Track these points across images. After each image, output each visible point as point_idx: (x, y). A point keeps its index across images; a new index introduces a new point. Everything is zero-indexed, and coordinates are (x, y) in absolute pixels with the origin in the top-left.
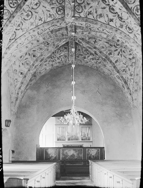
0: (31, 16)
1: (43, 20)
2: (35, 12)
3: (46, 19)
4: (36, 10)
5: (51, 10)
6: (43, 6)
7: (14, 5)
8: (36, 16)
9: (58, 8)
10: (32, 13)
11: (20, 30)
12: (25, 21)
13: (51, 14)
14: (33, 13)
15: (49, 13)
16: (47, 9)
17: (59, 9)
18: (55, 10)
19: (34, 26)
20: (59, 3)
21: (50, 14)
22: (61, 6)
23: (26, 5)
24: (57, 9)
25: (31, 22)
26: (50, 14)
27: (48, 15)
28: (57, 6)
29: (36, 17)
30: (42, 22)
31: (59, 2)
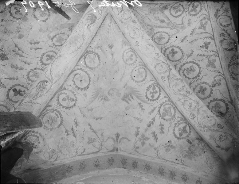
0: (194, 65)
1: (208, 40)
2: (190, 56)
3: (208, 35)
4: (185, 55)
5: (193, 26)
6: (182, 41)
7: (156, 92)
8: (198, 55)
9: (191, 13)
10: (187, 63)
11: (213, 88)
12: (200, 78)
13: (199, 25)
14: (189, 59)
15: (197, 31)
16: (189, 34)
17: (192, 11)
18: (193, 19)
19: (215, 60)
20: (183, 11)
21: (199, 28)
22: (188, 8)
23: (155, 67)
24: (192, 15)
25: (207, 66)
26: (199, 28)
27: (202, 30)
28: (188, 15)
29: (201, 55)
30: (212, 42)
31: (181, 12)
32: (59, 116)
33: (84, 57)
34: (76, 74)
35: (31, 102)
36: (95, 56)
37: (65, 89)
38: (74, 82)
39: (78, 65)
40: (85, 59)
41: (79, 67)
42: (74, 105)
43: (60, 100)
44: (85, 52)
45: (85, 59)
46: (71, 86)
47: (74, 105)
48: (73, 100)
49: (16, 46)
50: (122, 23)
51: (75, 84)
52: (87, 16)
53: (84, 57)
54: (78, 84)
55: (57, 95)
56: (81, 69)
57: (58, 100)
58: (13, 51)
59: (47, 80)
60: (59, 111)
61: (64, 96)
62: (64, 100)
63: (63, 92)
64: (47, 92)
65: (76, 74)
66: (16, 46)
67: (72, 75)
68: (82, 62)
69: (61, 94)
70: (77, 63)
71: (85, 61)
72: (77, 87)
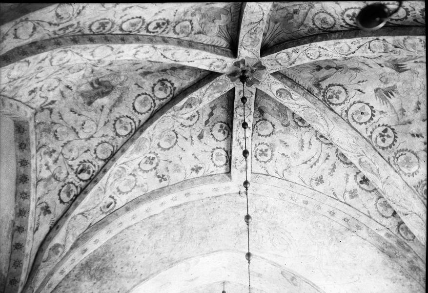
32: (404, 153)
33: (331, 106)
34: (353, 118)
35: (384, 183)
36: (330, 89)
37: (370, 137)
38: (362, 123)
39: (341, 114)
40: (333, 104)
41: (344, 113)
42: (393, 130)
43: (383, 145)
44: (324, 102)
45: (333, 104)
46: (367, 129)
47: (393, 130)
48: (385, 131)
49: (306, 163)
50: (293, 63)
51: (366, 123)
52: (280, 98)
53: (331, 106)
54: (365, 118)
55: (377, 148)
56: (346, 112)
57: (383, 148)
58: (311, 167)
59: (359, 158)
60: (397, 151)
61: (379, 139)
62: (384, 141)
63: (374, 140)
64: (374, 164)
65: (353, 118)
66: (306, 163)
67: (353, 124)
68: (338, 109)
69: (376, 142)
70: (339, 115)
71: (336, 105)
72: (369, 121)
